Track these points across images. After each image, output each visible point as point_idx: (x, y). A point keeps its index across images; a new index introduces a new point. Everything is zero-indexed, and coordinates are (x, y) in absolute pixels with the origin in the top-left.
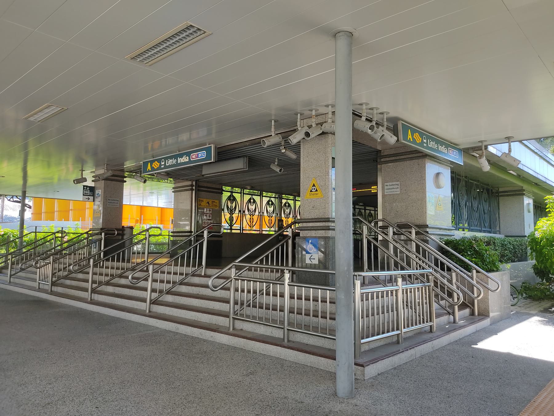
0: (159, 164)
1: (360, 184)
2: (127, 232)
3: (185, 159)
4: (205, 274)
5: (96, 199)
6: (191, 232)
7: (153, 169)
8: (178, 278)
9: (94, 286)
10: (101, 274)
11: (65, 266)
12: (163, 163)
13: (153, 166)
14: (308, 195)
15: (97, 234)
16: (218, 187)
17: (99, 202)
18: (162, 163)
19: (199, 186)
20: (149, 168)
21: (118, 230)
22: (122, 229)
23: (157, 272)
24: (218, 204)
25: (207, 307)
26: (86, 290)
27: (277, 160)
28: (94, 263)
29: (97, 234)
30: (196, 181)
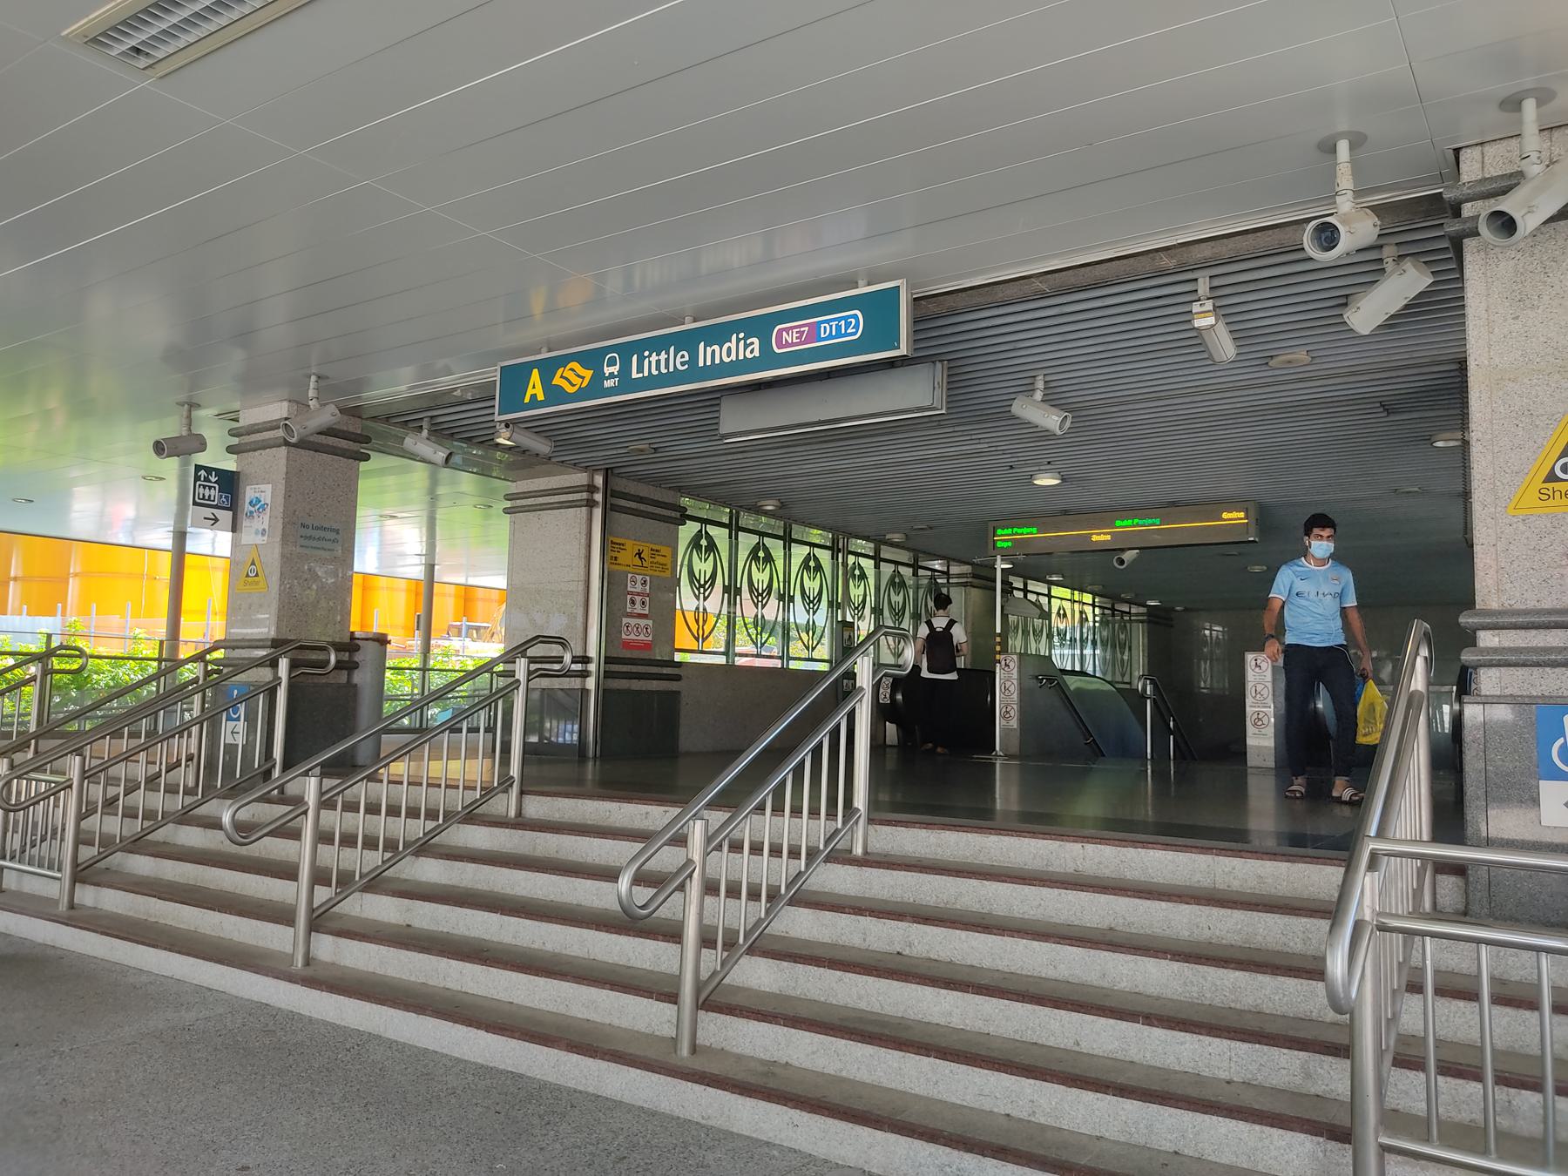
0: (588, 374)
1: (1173, 504)
2: (366, 655)
3: (737, 349)
4: (866, 852)
5: (246, 523)
6: (585, 660)
7: (554, 394)
8: (779, 871)
9: (323, 894)
10: (348, 840)
11: (112, 791)
12: (615, 369)
13: (557, 381)
14: (1532, 498)
15: (259, 663)
16: (668, 497)
17: (261, 530)
18: (607, 370)
19: (615, 494)
20: (535, 387)
21: (339, 647)
22: (351, 645)
23: (719, 847)
24: (667, 561)
25: (1029, 1037)
26: (284, 916)
27: (1040, 384)
28: (322, 794)
29: (259, 663)
30: (608, 473)
